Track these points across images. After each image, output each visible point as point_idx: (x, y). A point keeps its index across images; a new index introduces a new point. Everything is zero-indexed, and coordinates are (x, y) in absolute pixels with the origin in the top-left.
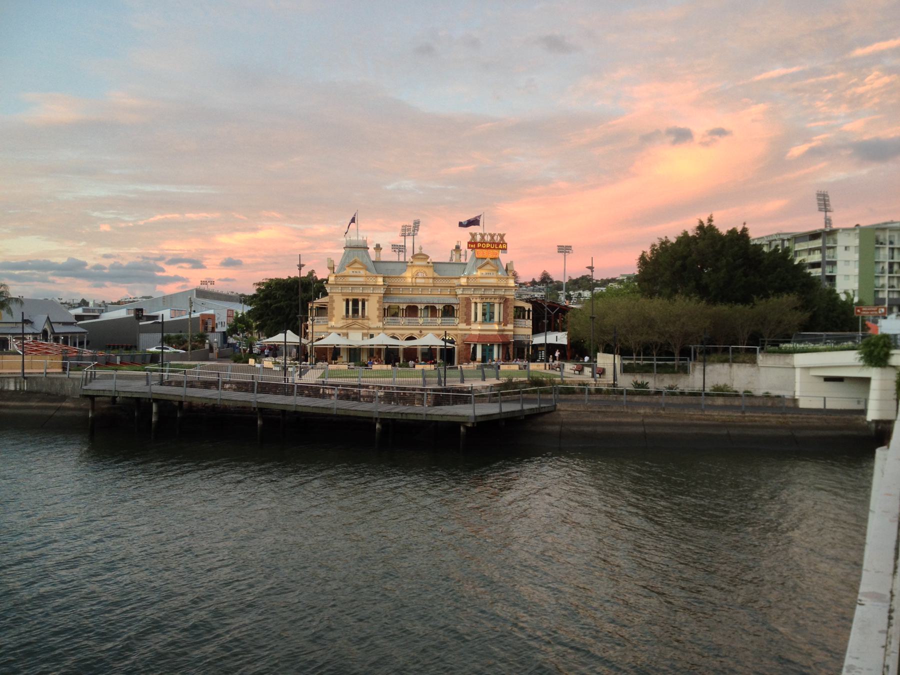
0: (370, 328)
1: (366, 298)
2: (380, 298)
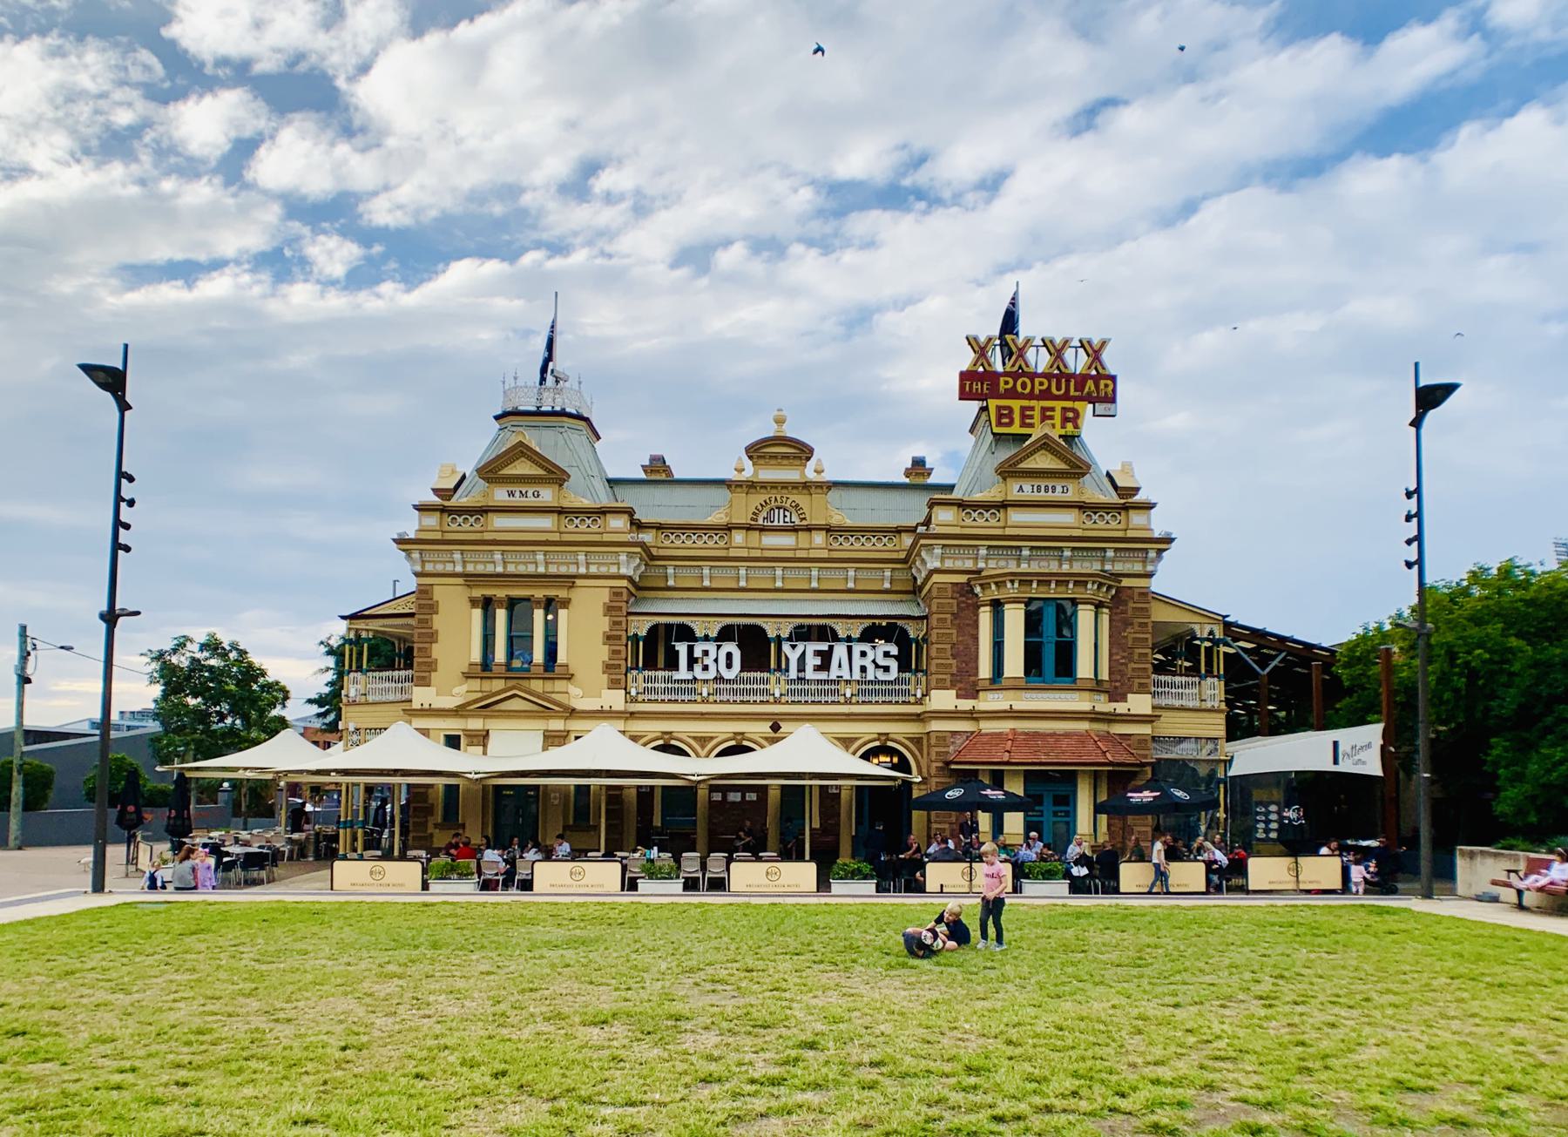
0: (572, 713)
1: (562, 594)
2: (616, 593)
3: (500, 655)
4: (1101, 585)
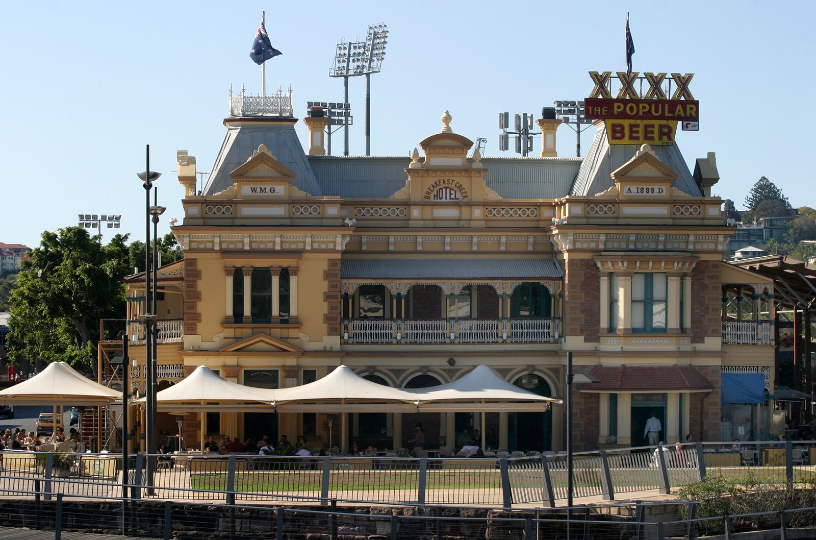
0: (305, 353)
2: (332, 263)
3: (247, 310)
4: (684, 264)
